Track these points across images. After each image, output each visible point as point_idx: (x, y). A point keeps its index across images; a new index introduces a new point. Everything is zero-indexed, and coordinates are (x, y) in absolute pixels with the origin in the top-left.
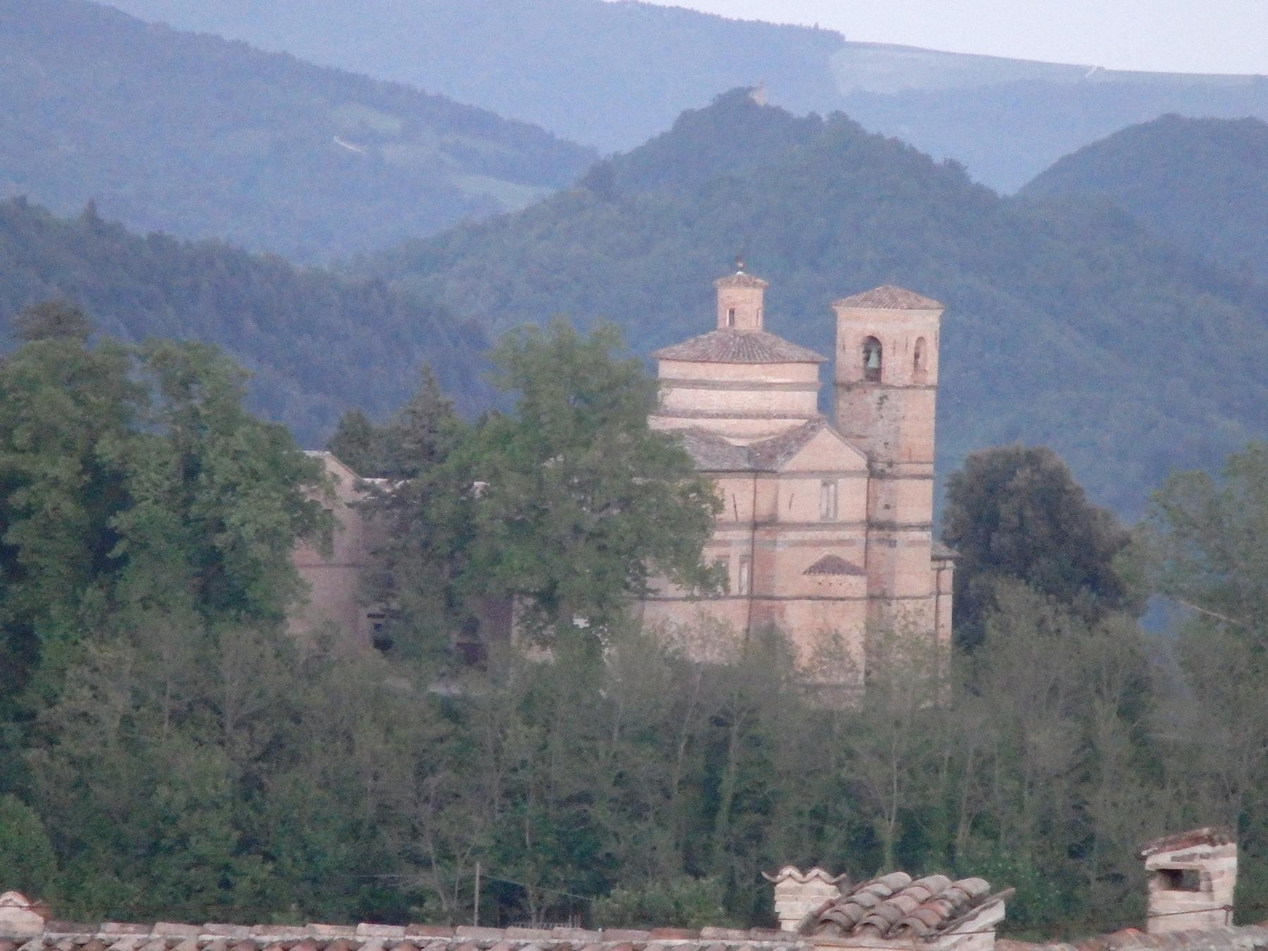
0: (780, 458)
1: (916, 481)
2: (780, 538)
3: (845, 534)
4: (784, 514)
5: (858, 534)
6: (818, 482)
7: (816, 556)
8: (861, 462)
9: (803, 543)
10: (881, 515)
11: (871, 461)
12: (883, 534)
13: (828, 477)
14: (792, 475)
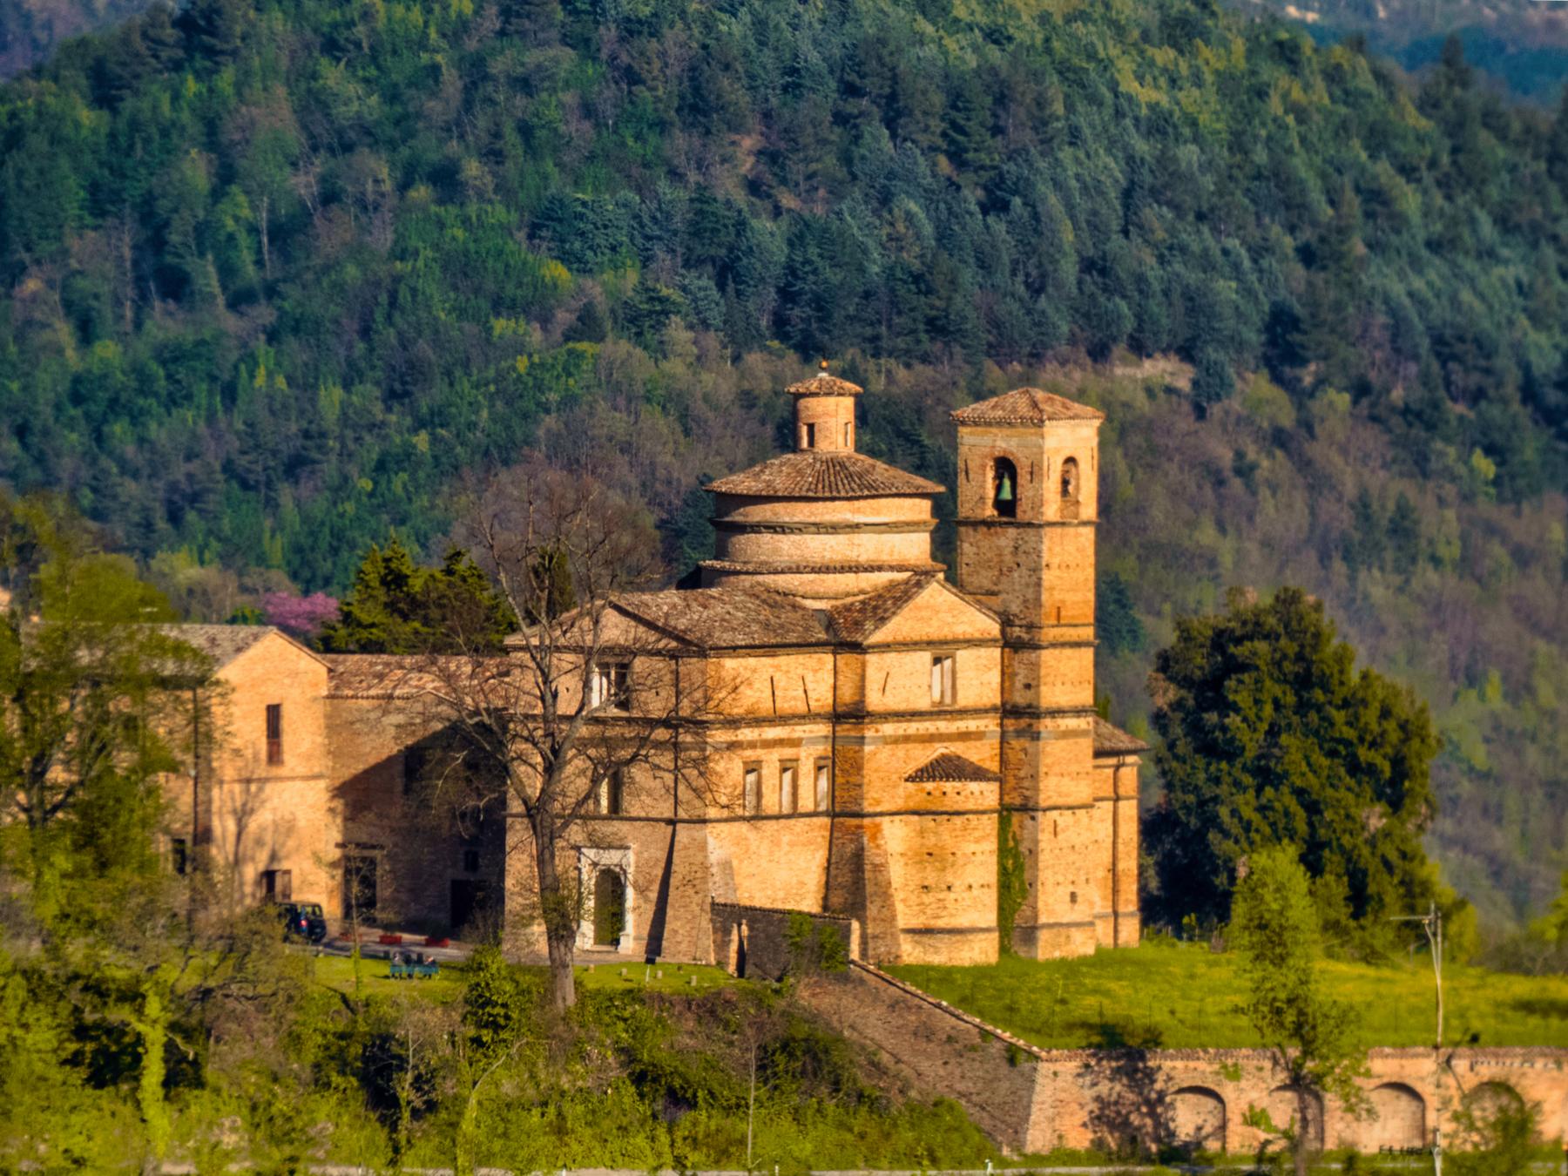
0: (869, 625)
1: (1068, 652)
2: (869, 733)
3: (972, 724)
4: (875, 700)
5: (990, 724)
6: (926, 656)
7: (924, 755)
8: (993, 628)
9: (907, 739)
10: (1020, 698)
11: (1006, 621)
12: (1024, 722)
13: (941, 650)
14: (885, 647)
